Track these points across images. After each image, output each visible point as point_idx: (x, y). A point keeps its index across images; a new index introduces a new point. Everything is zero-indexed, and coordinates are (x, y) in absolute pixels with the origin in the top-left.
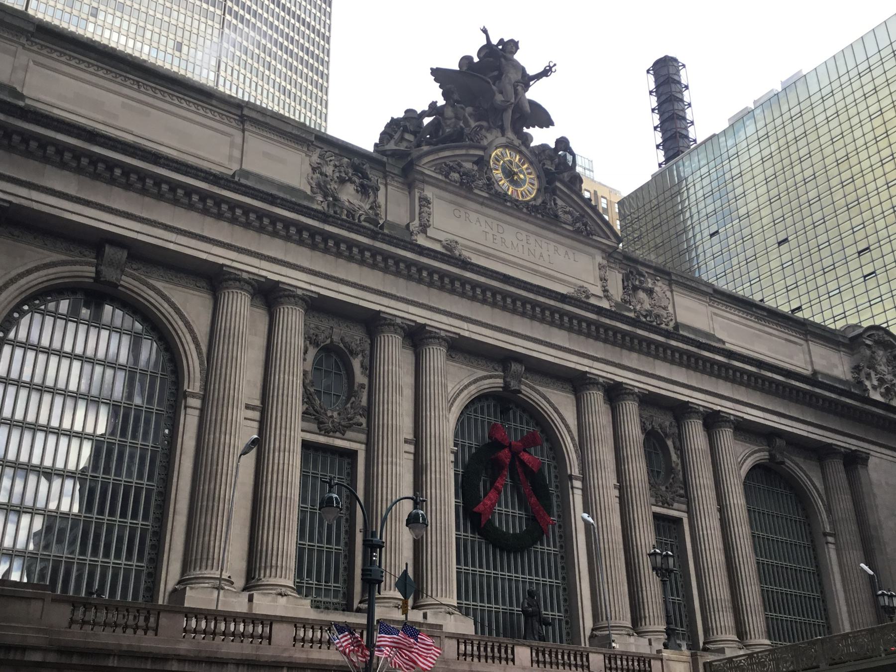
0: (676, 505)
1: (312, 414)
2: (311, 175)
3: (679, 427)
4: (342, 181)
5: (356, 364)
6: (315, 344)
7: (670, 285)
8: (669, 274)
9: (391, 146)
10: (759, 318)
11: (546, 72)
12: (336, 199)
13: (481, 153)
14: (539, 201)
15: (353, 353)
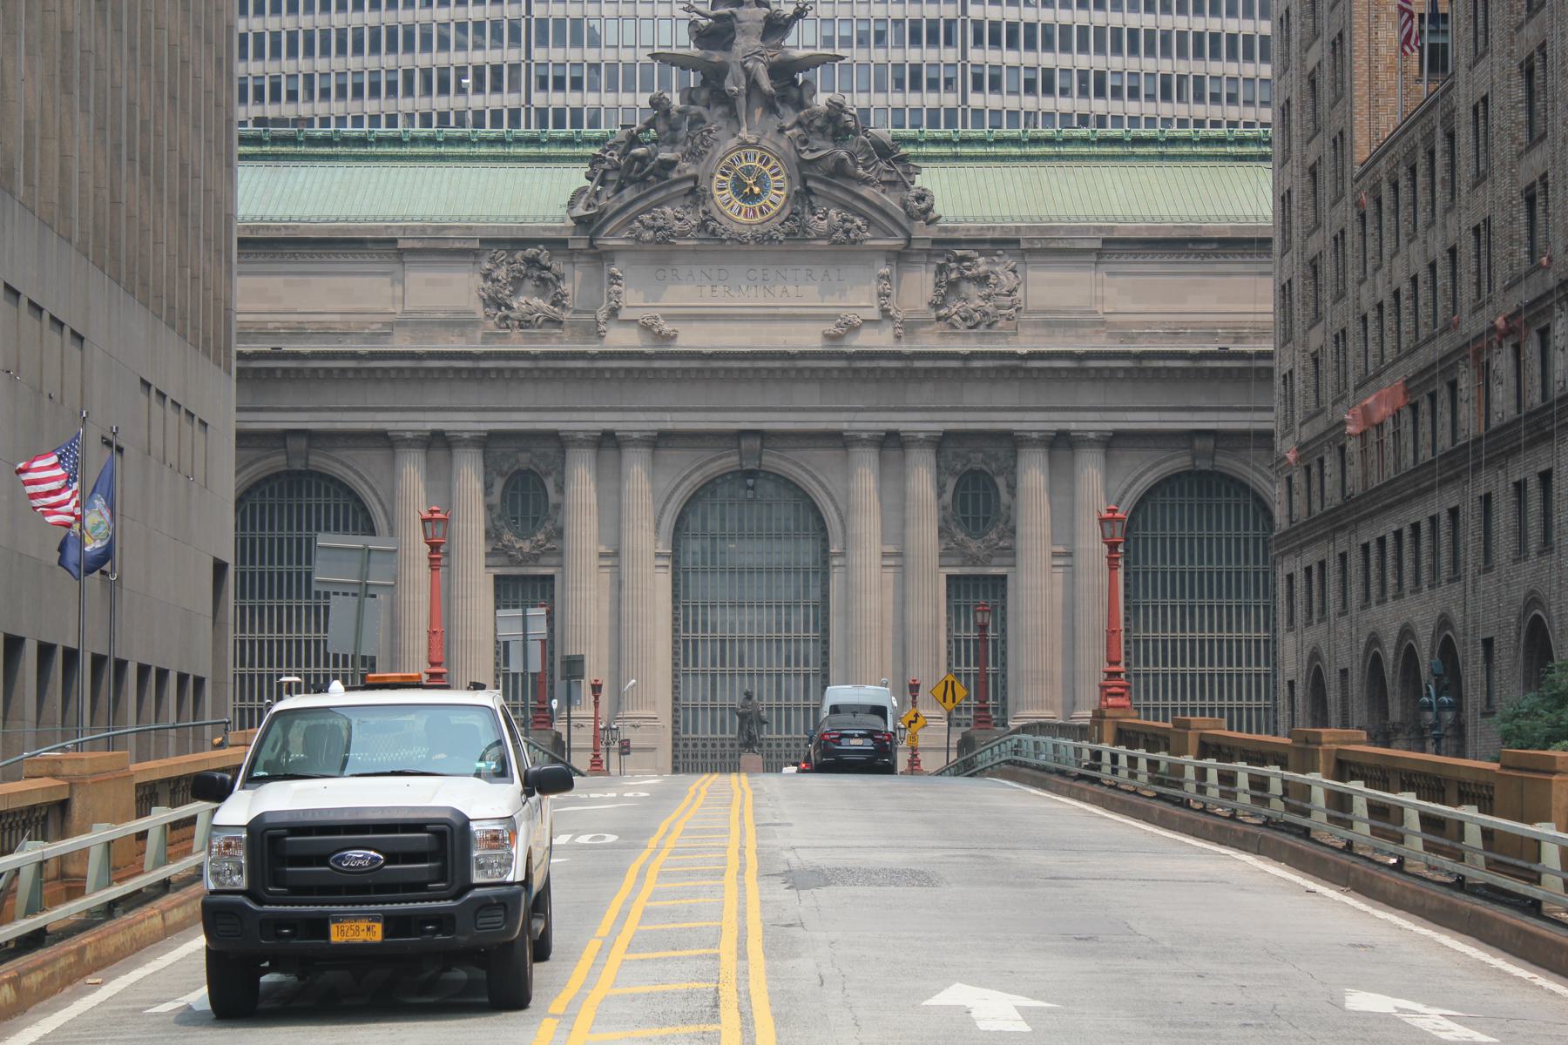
0: (995, 560)
1: (497, 550)
2: (481, 283)
3: (1015, 457)
4: (517, 283)
5: (550, 484)
6: (501, 474)
7: (1023, 256)
8: (1017, 241)
9: (580, 211)
10: (1207, 255)
11: (800, 14)
12: (509, 307)
13: (691, 184)
14: (786, 213)
15: (548, 474)
